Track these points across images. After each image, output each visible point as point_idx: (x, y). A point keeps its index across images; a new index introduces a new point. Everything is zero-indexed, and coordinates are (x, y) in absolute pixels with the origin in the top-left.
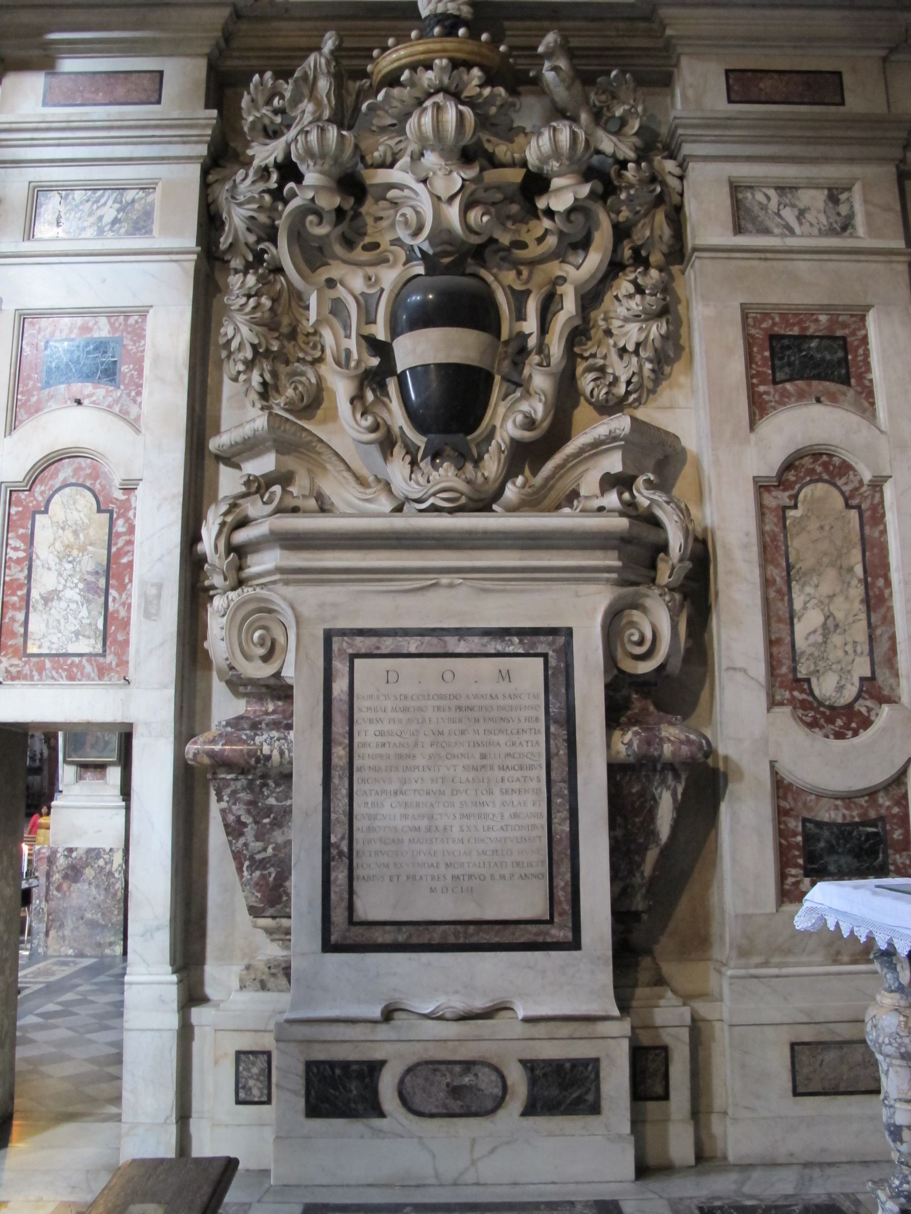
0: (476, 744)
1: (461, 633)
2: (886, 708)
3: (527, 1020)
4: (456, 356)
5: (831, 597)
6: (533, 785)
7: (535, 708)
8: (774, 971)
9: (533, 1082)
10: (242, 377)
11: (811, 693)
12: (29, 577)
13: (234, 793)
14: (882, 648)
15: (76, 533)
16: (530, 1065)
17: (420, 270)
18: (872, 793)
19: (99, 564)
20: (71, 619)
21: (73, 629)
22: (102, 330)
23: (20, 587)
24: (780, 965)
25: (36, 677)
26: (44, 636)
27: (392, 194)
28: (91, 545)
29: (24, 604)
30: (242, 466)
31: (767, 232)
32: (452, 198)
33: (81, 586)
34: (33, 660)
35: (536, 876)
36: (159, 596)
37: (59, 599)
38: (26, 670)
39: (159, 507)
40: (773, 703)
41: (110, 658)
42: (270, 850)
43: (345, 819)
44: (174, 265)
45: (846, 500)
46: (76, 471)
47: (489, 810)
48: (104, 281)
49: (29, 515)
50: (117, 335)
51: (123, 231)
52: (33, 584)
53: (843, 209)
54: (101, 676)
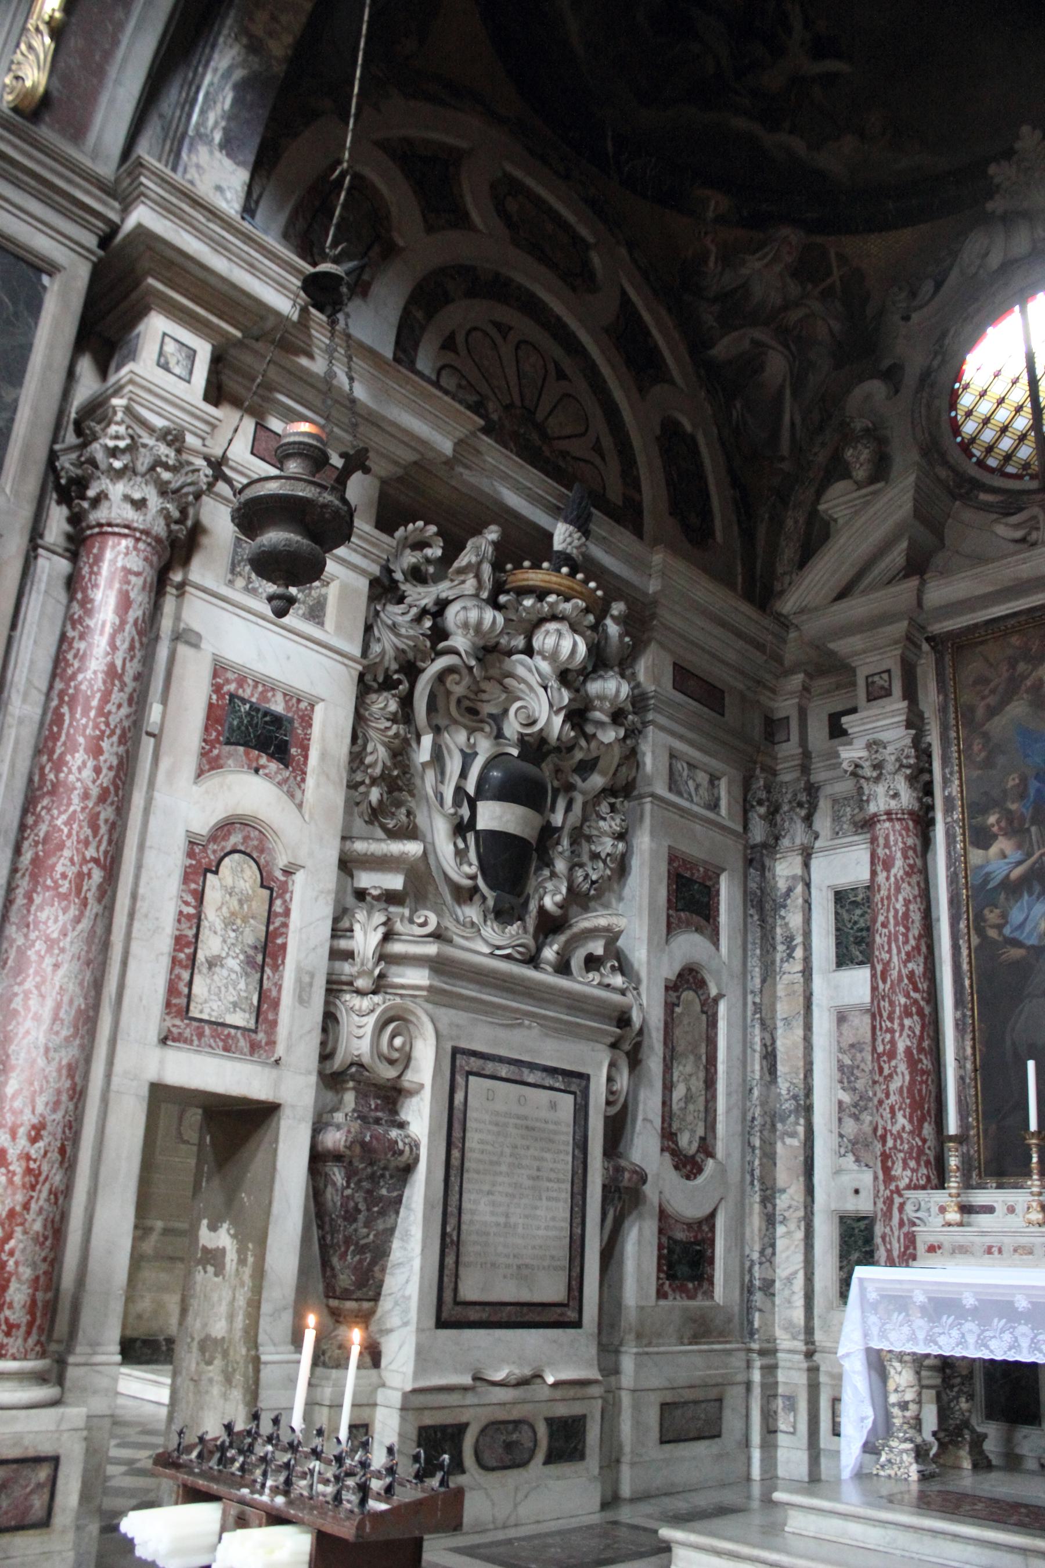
0: (535, 1158)
1: (532, 1066)
2: (710, 1162)
3: (556, 1385)
4: (512, 828)
5: (690, 1075)
6: (473, 1197)
7: (567, 1134)
8: (656, 1349)
9: (551, 1436)
10: (362, 789)
11: (677, 1144)
12: (197, 936)
13: (360, 1181)
14: (710, 1119)
15: (241, 902)
16: (550, 1421)
17: (515, 752)
18: (699, 1223)
19: (258, 939)
20: (231, 989)
21: (232, 999)
22: (278, 706)
23: (188, 945)
24: (658, 1345)
25: (196, 1042)
26: (206, 1002)
27: (508, 681)
28: (253, 918)
29: (190, 963)
30: (355, 873)
31: (680, 794)
32: (560, 710)
33: (242, 957)
34: (195, 1024)
35: (555, 1268)
36: (311, 985)
37: (222, 966)
38: (187, 1033)
39: (316, 899)
40: (662, 1150)
41: (261, 1036)
42: (371, 1237)
43: (455, 1211)
44: (343, 667)
45: (703, 1005)
46: (246, 839)
47: (538, 1212)
48: (288, 658)
49: (201, 871)
50: (290, 715)
51: (301, 612)
52: (200, 945)
53: (716, 791)
54: (252, 1052)
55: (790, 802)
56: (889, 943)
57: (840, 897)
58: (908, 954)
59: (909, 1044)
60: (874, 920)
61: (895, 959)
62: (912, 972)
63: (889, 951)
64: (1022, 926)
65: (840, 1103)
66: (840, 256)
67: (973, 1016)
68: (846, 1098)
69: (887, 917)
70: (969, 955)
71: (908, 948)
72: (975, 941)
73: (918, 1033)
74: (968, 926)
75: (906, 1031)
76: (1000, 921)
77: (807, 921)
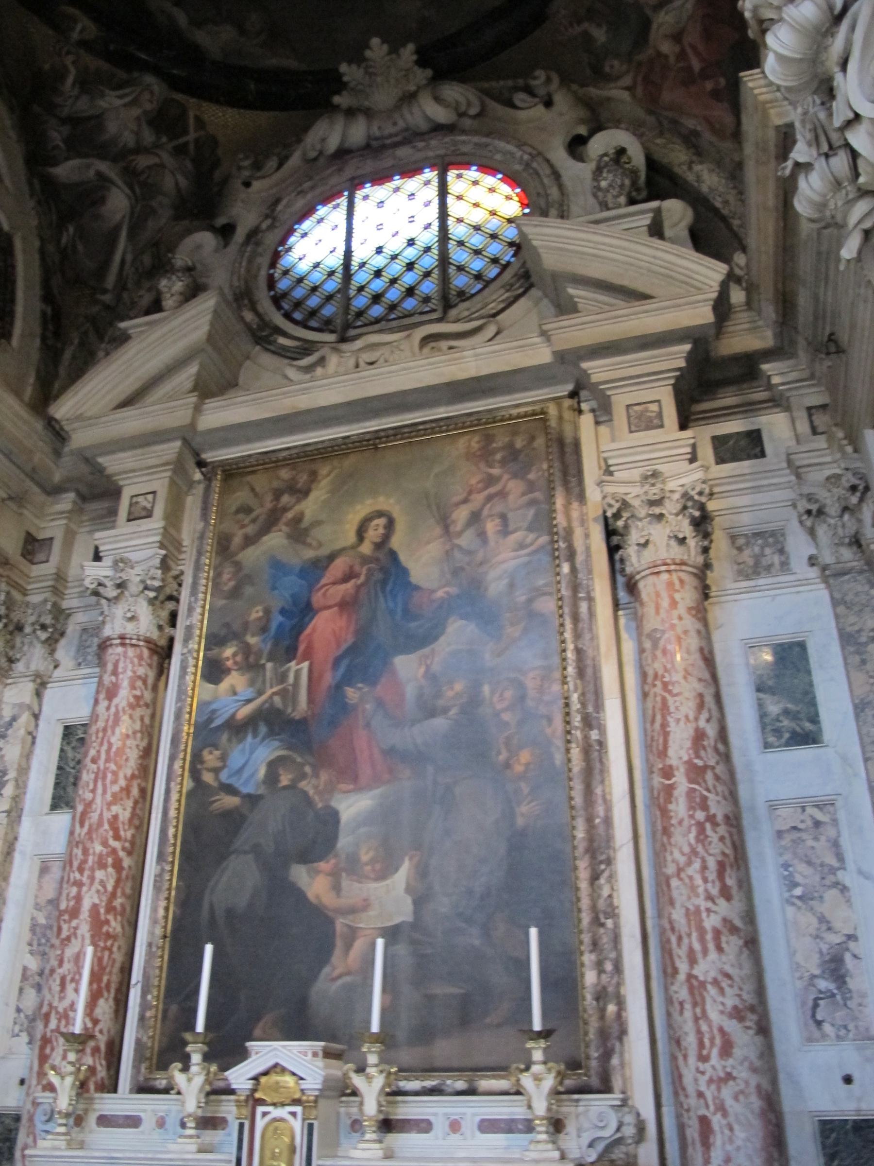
55: (33, 624)
56: (95, 781)
57: (68, 732)
58: (114, 795)
59: (97, 901)
60: (86, 755)
61: (99, 800)
62: (116, 817)
63: (93, 791)
64: (240, 771)
65: (25, 969)
66: (198, 119)
67: (172, 871)
68: (33, 964)
69: (99, 752)
70: (179, 801)
71: (116, 788)
72: (188, 784)
73: (110, 888)
74: (183, 768)
75: (97, 886)
76: (219, 764)
77: (28, 756)
